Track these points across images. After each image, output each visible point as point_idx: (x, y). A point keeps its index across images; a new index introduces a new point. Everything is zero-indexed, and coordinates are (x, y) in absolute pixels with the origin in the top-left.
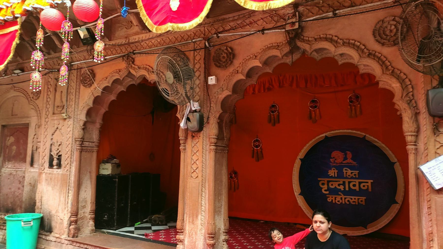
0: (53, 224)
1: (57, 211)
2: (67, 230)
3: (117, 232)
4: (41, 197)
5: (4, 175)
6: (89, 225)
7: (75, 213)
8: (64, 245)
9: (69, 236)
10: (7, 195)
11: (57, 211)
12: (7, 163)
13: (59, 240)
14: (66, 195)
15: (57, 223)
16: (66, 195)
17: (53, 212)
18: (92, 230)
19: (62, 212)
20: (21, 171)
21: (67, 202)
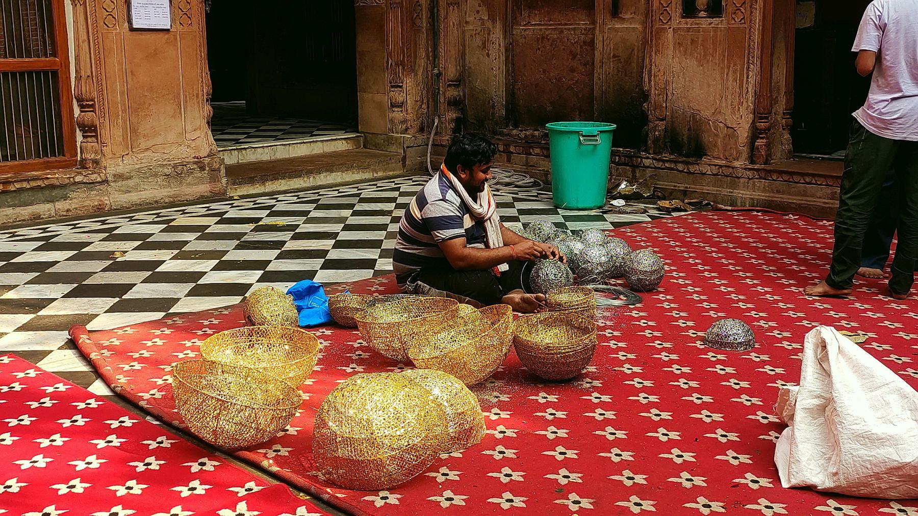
0: (706, 138)
1: (717, 111)
2: (745, 150)
3: (834, 156)
4: (667, 83)
5: (522, 41)
6: (784, 142)
7: (760, 114)
8: (742, 180)
9: (752, 162)
10: (537, 85)
11: (717, 111)
12: (525, 13)
13: (728, 171)
14: (742, 75)
15: (716, 135)
16: (742, 75)
17: (706, 113)
18: (790, 152)
19: (733, 113)
20: (574, 29)
21: (744, 92)
